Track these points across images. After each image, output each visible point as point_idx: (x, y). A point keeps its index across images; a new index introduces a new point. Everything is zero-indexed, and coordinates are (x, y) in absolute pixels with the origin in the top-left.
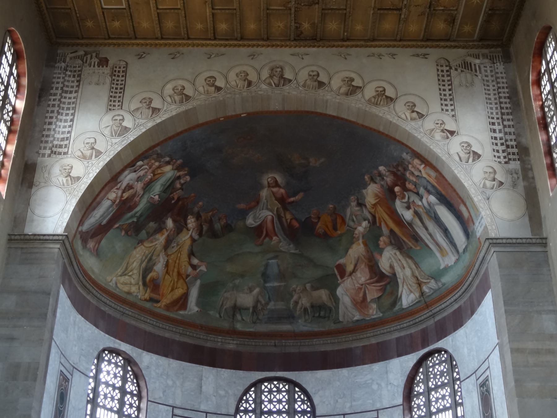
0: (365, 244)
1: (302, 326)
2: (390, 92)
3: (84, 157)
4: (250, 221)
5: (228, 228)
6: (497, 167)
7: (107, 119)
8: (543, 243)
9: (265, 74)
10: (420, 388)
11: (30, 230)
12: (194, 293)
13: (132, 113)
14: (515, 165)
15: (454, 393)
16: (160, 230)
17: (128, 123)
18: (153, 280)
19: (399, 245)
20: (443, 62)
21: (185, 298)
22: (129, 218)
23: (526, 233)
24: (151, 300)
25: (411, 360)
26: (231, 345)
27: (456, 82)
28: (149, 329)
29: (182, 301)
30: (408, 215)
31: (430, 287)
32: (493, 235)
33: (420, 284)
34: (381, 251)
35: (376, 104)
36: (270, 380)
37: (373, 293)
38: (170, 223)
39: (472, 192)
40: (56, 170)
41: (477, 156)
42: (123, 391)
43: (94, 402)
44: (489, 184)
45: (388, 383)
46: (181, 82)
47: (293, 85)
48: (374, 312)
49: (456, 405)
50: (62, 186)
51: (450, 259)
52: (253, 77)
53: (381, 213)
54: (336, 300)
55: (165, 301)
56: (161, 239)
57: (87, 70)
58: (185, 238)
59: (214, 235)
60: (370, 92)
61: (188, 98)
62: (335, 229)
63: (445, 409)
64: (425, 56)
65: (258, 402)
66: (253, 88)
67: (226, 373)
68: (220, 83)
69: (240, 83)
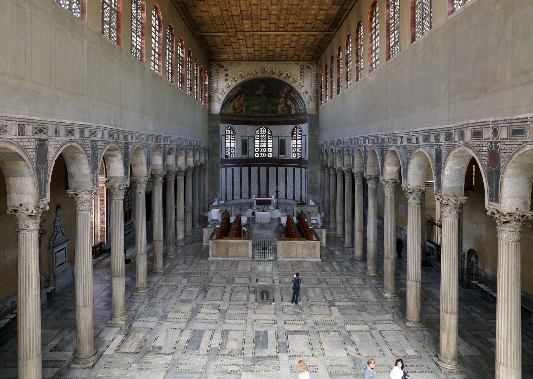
0: (284, 99)
1: (270, 114)
2: (289, 75)
3: (221, 94)
4: (257, 93)
5: (252, 94)
6: (312, 96)
7: (225, 83)
8: (318, 115)
9: (260, 70)
10: (295, 133)
11: (212, 112)
12: (244, 109)
13: (231, 81)
14: (315, 95)
15: (301, 137)
16: (236, 99)
17: (230, 84)
18: (235, 108)
19: (292, 101)
20: (302, 66)
21: (242, 110)
22: (230, 99)
23: (315, 113)
24: (235, 112)
25: (293, 126)
26: (253, 119)
27: (304, 72)
28: (235, 119)
29: (242, 111)
30: (294, 96)
31: (298, 111)
32: (308, 113)
33: (296, 110)
34: (288, 101)
35: (286, 79)
36: (262, 127)
37: (286, 109)
38: (239, 96)
39: (305, 102)
40: (216, 97)
41: (307, 92)
42: (231, 135)
43: (226, 140)
44: (309, 100)
45: (288, 131)
46: (241, 73)
47: (267, 73)
48: (286, 113)
49: (301, 139)
50: (218, 102)
51: (302, 108)
52: (258, 71)
53: (287, 94)
54: (278, 109)
55: (238, 112)
56: (237, 100)
57: (219, 69)
58: (242, 98)
59: (248, 96)
60: (284, 75)
61: (243, 77)
62: (277, 95)
63: (299, 139)
64: (298, 64)
65: (260, 132)
66: (258, 74)
67: (252, 126)
68: (250, 73)
69: (255, 73)
